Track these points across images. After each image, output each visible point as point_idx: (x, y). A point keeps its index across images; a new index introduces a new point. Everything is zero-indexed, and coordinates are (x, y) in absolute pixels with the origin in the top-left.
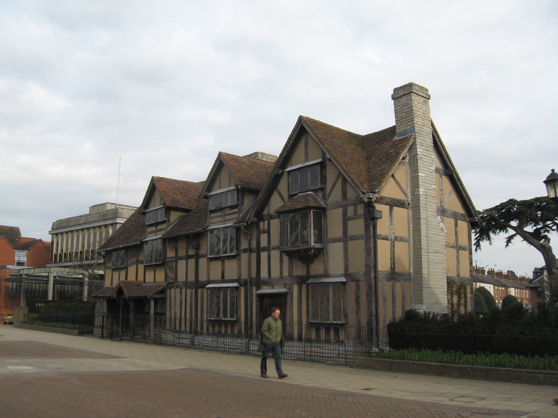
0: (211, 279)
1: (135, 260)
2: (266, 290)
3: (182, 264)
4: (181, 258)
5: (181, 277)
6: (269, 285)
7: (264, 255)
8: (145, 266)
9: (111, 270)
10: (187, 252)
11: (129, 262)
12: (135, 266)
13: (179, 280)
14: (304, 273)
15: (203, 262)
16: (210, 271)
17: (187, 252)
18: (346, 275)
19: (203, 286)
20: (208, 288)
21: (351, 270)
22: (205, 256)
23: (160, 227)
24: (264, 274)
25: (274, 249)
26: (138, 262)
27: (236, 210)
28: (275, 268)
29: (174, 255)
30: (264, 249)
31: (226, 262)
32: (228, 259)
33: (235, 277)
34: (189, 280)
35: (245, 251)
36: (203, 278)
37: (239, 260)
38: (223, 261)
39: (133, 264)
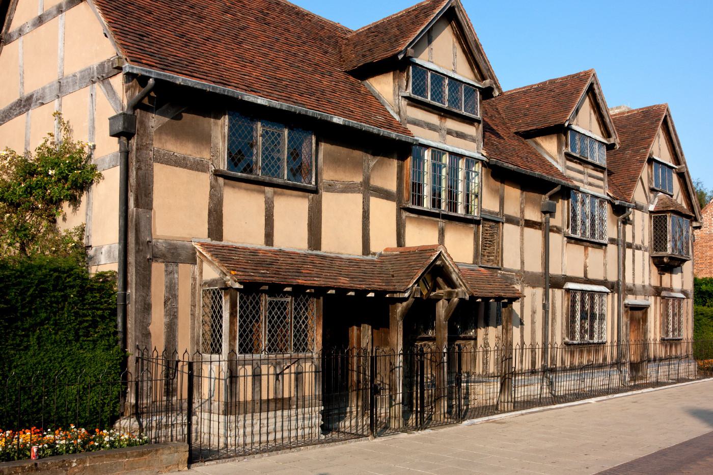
0: (569, 274)
1: (359, 179)
2: (631, 300)
3: (510, 232)
4: (511, 220)
5: (511, 261)
6: (633, 294)
7: (629, 252)
8: (401, 209)
9: (205, 179)
10: (522, 211)
11: (328, 175)
12: (359, 197)
13: (506, 265)
14: (659, 285)
15: (555, 238)
16: (568, 260)
17: (522, 211)
18: (683, 292)
19: (557, 283)
20: (568, 290)
21: (685, 288)
22: (558, 230)
23: (451, 124)
24: (629, 280)
25: (638, 248)
26: (369, 190)
27: (600, 175)
28: (640, 271)
29: (497, 209)
30: (630, 246)
31: (590, 249)
32: (593, 247)
33: (602, 278)
34: (526, 269)
35: (612, 241)
36: (554, 270)
37: (605, 251)
38: (586, 248)
39: (348, 188)
